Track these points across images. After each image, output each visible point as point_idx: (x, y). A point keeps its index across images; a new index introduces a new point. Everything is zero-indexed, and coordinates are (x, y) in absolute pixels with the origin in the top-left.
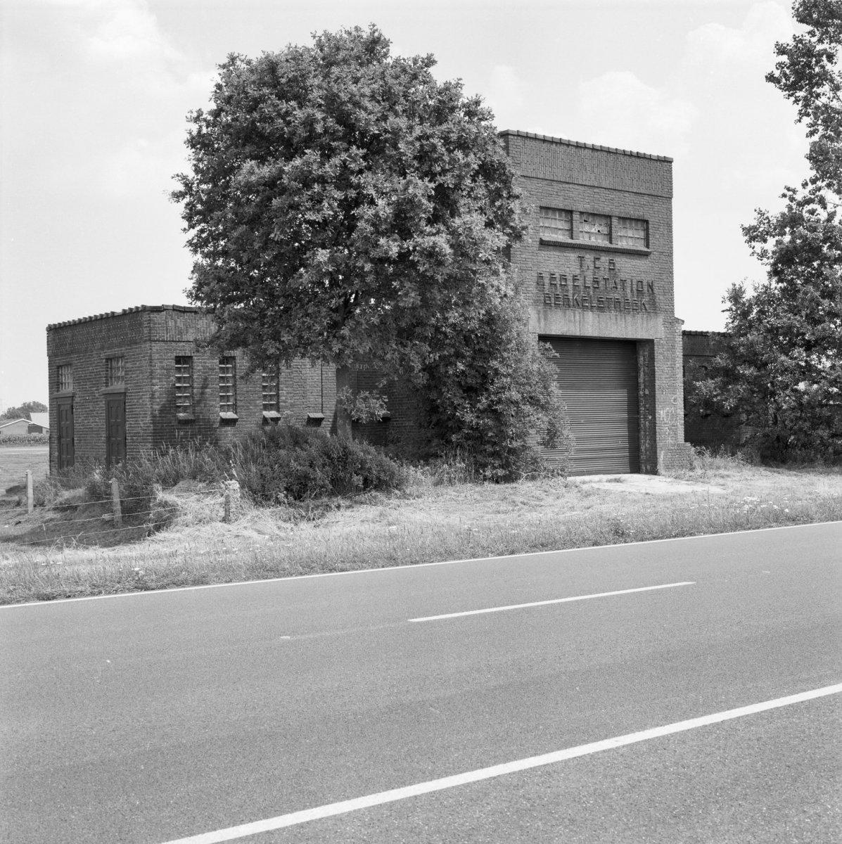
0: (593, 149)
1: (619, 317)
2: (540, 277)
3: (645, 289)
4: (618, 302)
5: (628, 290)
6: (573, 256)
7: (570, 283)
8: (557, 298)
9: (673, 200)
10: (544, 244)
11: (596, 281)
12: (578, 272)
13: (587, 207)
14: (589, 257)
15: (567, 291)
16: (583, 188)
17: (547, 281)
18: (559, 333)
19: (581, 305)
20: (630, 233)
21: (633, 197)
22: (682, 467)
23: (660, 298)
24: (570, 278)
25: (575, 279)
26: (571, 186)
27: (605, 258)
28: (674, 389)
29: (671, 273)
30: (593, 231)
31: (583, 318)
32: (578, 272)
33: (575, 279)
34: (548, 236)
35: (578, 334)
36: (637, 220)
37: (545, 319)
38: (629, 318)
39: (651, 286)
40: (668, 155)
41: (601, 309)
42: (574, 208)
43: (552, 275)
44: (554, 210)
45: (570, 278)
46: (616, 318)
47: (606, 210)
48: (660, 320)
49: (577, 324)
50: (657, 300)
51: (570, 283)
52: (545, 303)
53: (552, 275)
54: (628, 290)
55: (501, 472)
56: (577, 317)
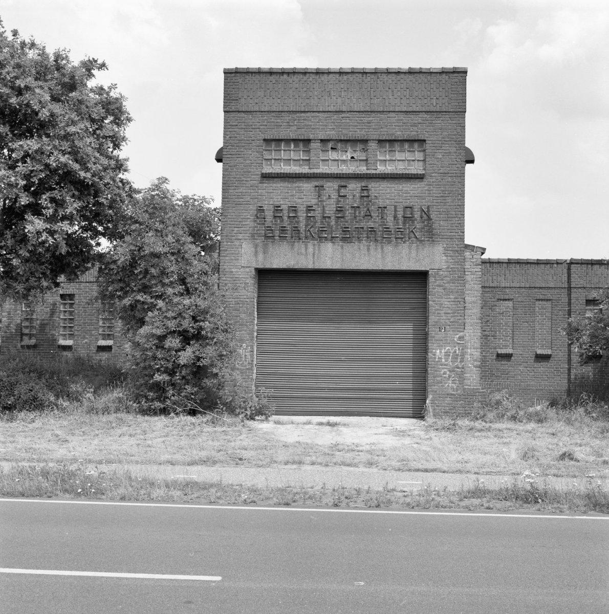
0: (341, 73)
1: (372, 251)
2: (261, 210)
3: (417, 215)
4: (372, 230)
5: (390, 218)
6: (307, 186)
7: (302, 215)
8: (283, 230)
10: (266, 177)
11: (340, 210)
12: (314, 201)
13: (332, 134)
14: (331, 187)
15: (298, 222)
16: (326, 115)
17: (269, 215)
18: (284, 266)
19: (321, 236)
20: (398, 156)
21: (402, 116)
22: (466, 414)
23: (439, 224)
25: (309, 209)
26: (308, 114)
27: (354, 187)
30: (344, 158)
31: (319, 250)
32: (314, 201)
33: (309, 209)
34: (267, 170)
36: (411, 141)
38: (389, 248)
39: (426, 215)
40: (459, 65)
41: (344, 239)
42: (311, 137)
43: (277, 209)
44: (288, 141)
46: (368, 249)
47: (359, 134)
48: (439, 249)
49: (310, 257)
50: (435, 226)
51: (302, 215)
52: (266, 237)
53: (277, 209)
54: (390, 218)
55: (158, 405)
56: (311, 249)
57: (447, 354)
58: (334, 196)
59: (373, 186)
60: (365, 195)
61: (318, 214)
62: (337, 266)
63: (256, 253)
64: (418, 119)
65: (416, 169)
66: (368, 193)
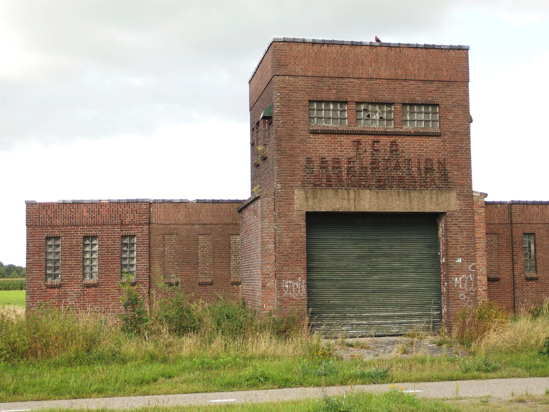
2: (309, 160)
4: (401, 179)
5: (415, 169)
6: (346, 140)
9: (470, 84)
10: (315, 132)
17: (317, 163)
23: (453, 173)
24: (344, 160)
26: (344, 80)
28: (470, 258)
29: (467, 151)
31: (359, 196)
35: (353, 210)
37: (315, 198)
38: (414, 194)
42: (349, 99)
43: (323, 161)
45: (344, 160)
46: (399, 194)
48: (454, 194)
49: (352, 201)
50: (450, 175)
56: (352, 196)
57: (463, 281)
58: (369, 149)
59: (399, 140)
60: (394, 148)
61: (357, 165)
62: (374, 209)
63: (307, 199)
64: (433, 87)
65: (435, 128)
66: (396, 147)
